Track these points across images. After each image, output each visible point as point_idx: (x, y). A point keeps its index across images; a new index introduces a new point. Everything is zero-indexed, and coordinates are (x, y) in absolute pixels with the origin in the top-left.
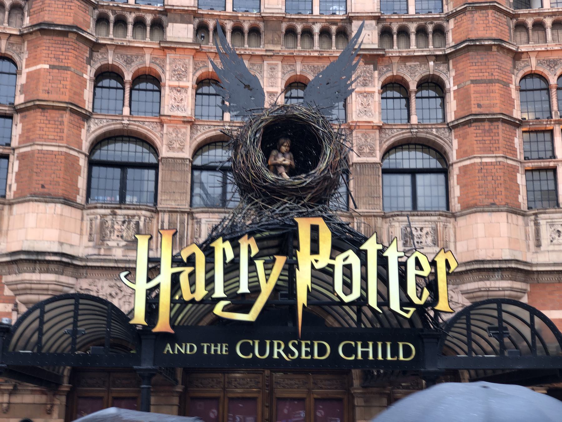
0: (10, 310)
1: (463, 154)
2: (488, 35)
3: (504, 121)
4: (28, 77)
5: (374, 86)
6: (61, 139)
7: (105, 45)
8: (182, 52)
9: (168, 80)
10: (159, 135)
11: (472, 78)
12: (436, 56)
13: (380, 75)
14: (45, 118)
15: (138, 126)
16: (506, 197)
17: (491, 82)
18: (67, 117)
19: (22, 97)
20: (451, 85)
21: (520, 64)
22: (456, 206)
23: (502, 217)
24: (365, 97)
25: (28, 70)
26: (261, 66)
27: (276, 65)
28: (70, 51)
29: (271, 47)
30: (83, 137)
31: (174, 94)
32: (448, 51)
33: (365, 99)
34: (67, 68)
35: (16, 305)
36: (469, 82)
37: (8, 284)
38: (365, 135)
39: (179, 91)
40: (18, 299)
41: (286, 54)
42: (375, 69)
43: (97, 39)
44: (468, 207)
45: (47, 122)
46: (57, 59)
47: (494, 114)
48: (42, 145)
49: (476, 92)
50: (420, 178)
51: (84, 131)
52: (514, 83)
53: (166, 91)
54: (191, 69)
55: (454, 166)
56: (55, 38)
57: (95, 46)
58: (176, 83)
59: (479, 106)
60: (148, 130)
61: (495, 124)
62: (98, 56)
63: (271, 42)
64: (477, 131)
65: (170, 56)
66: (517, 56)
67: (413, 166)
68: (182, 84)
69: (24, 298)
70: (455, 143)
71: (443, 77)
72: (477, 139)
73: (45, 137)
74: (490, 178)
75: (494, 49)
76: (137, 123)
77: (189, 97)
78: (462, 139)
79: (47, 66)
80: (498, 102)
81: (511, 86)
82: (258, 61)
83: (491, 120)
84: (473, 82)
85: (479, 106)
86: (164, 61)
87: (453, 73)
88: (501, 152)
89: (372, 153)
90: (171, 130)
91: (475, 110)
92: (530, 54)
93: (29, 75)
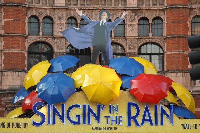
0: (4, 110)
1: (168, 50)
2: (179, 3)
3: (183, 37)
4: (5, 23)
5: (135, 22)
6: (19, 48)
7: (32, 8)
8: (61, 10)
9: (56, 21)
10: (53, 43)
11: (172, 20)
12: (160, 9)
13: (138, 17)
14: (13, 40)
15: (46, 39)
16: (183, 67)
17: (179, 22)
18: (21, 39)
19: (3, 31)
20: (165, 22)
21: (192, 12)
22: (165, 69)
23: (180, 74)
24: (132, 26)
25: (4, 20)
26: (92, 14)
27: (98, 13)
28: (20, 13)
29: (95, 6)
30: (26, 45)
31: (59, 27)
32: (164, 8)
33: (132, 27)
34: (19, 20)
35: (6, 108)
36: (171, 22)
37: (3, 101)
38: (132, 42)
39: (60, 25)
40: (7, 106)
41: (101, 9)
42: (136, 15)
43: (29, 6)
44: (169, 71)
45: (14, 41)
46: (16, 16)
47: (180, 35)
48: (13, 50)
49: (173, 26)
50: (153, 56)
51: (26, 43)
52: (189, 21)
53: (56, 26)
54: (65, 16)
55: (165, 54)
56: (14, 8)
57: (29, 8)
58: (59, 22)
59: (174, 31)
60: (49, 41)
61: (180, 38)
62: (29, 12)
63: (95, 3)
64: (173, 41)
65: (57, 11)
66: (191, 9)
67: (150, 52)
68: (61, 22)
69: (9, 105)
70: (166, 44)
71: (162, 17)
72: (173, 44)
73: (14, 47)
74: (177, 60)
75: (181, 8)
76: (45, 38)
77: (64, 27)
78: (168, 43)
79: (12, 20)
80: (181, 30)
81: (188, 22)
82: (90, 12)
83: (178, 37)
84: (172, 22)
85: (174, 31)
86: (54, 13)
87: (166, 17)
88: (181, 49)
89: (134, 49)
90: (58, 41)
91: (173, 33)
92: (196, 9)
93: (5, 22)
